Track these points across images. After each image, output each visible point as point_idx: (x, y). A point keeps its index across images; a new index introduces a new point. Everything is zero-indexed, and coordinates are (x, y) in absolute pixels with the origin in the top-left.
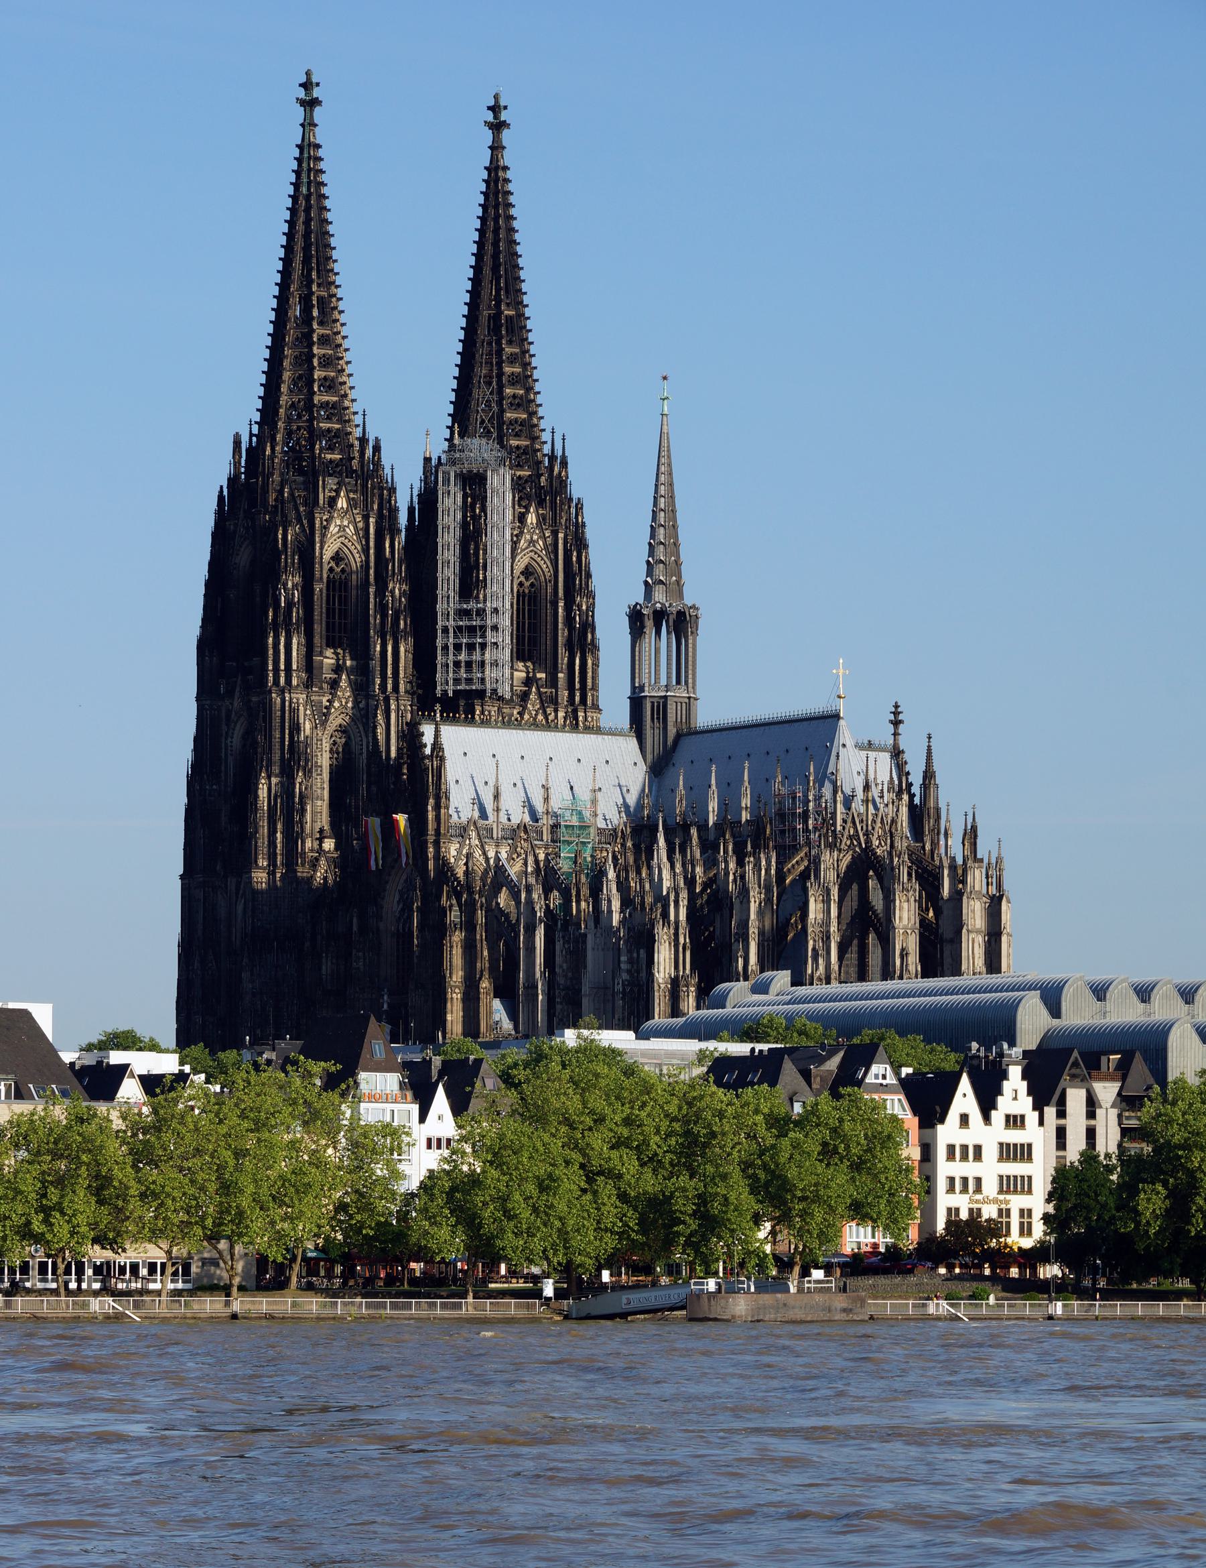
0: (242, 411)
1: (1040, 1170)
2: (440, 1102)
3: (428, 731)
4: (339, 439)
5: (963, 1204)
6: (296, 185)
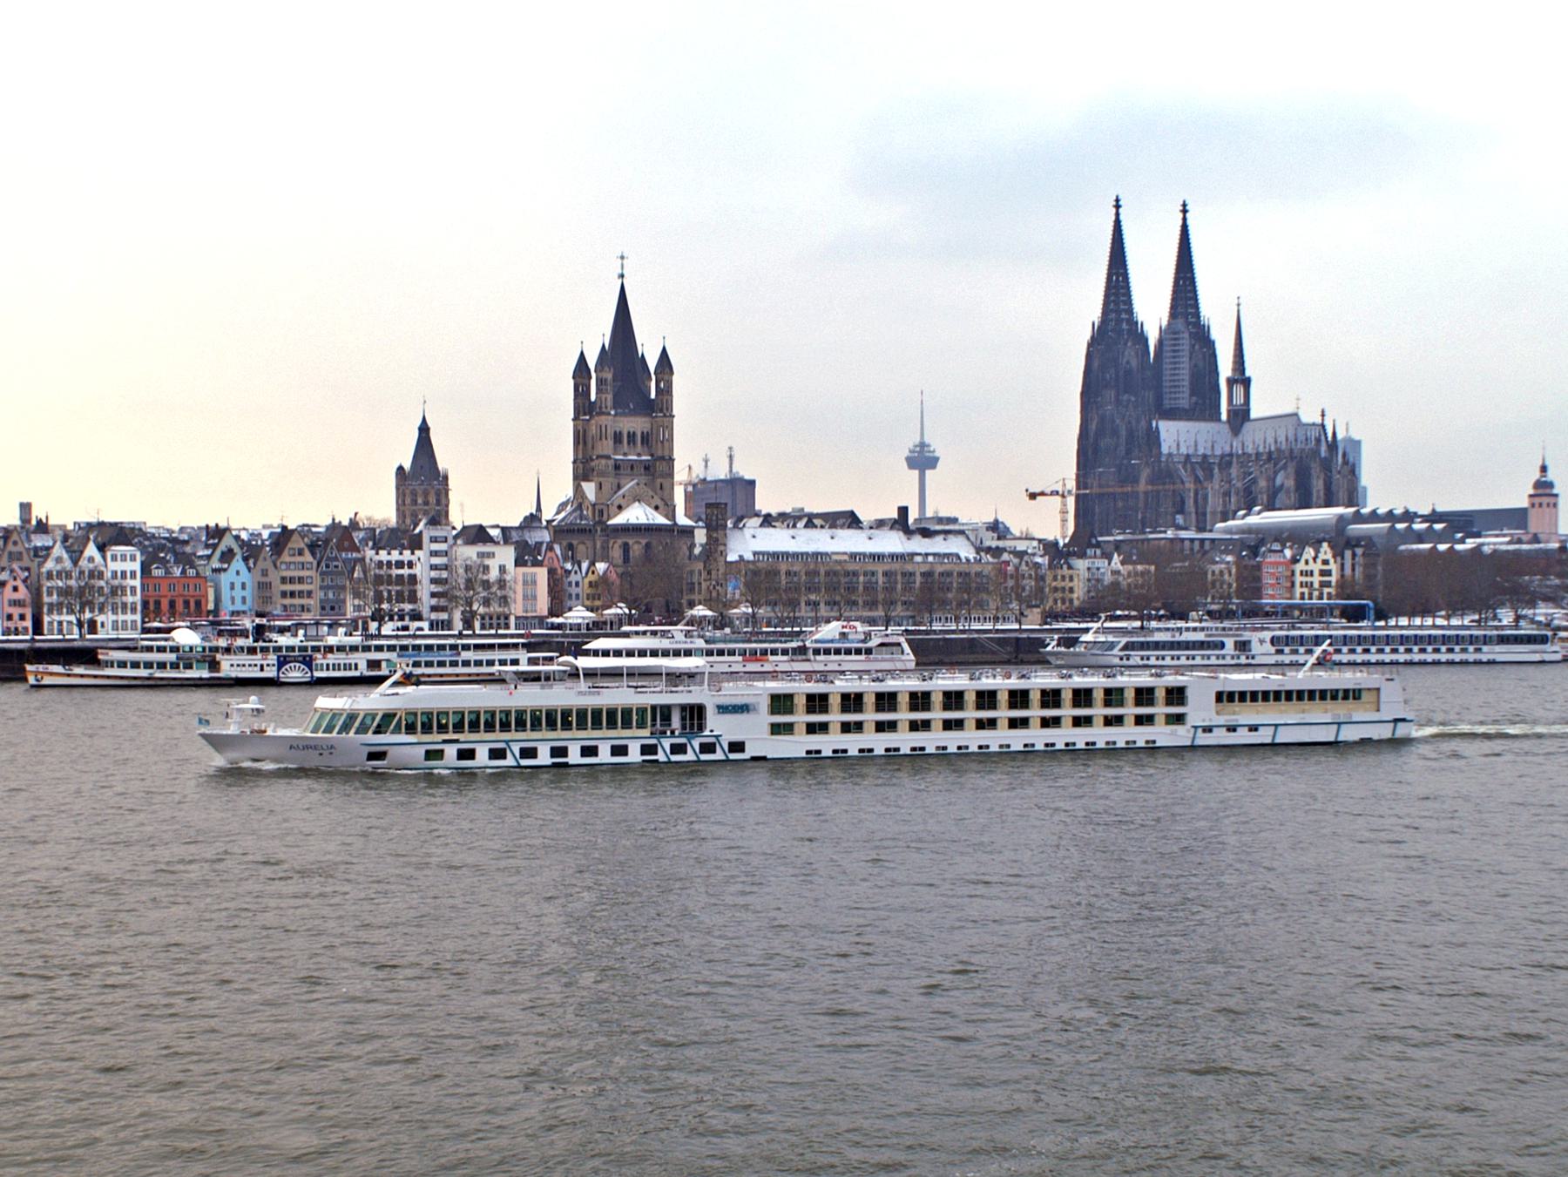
0: (1094, 311)
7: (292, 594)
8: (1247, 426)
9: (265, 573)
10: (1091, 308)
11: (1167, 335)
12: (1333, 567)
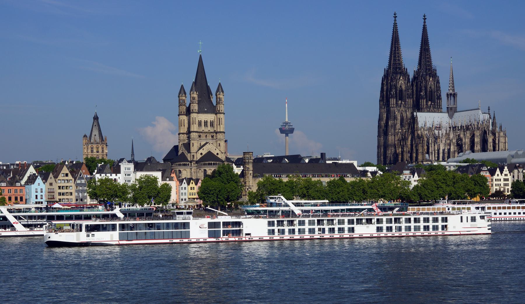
0: (386, 65)
1: (510, 183)
2: (416, 174)
3: (415, 113)
4: (400, 69)
5: (498, 188)
8: (456, 115)
9: (51, 184)
10: (383, 63)
12: (509, 177)
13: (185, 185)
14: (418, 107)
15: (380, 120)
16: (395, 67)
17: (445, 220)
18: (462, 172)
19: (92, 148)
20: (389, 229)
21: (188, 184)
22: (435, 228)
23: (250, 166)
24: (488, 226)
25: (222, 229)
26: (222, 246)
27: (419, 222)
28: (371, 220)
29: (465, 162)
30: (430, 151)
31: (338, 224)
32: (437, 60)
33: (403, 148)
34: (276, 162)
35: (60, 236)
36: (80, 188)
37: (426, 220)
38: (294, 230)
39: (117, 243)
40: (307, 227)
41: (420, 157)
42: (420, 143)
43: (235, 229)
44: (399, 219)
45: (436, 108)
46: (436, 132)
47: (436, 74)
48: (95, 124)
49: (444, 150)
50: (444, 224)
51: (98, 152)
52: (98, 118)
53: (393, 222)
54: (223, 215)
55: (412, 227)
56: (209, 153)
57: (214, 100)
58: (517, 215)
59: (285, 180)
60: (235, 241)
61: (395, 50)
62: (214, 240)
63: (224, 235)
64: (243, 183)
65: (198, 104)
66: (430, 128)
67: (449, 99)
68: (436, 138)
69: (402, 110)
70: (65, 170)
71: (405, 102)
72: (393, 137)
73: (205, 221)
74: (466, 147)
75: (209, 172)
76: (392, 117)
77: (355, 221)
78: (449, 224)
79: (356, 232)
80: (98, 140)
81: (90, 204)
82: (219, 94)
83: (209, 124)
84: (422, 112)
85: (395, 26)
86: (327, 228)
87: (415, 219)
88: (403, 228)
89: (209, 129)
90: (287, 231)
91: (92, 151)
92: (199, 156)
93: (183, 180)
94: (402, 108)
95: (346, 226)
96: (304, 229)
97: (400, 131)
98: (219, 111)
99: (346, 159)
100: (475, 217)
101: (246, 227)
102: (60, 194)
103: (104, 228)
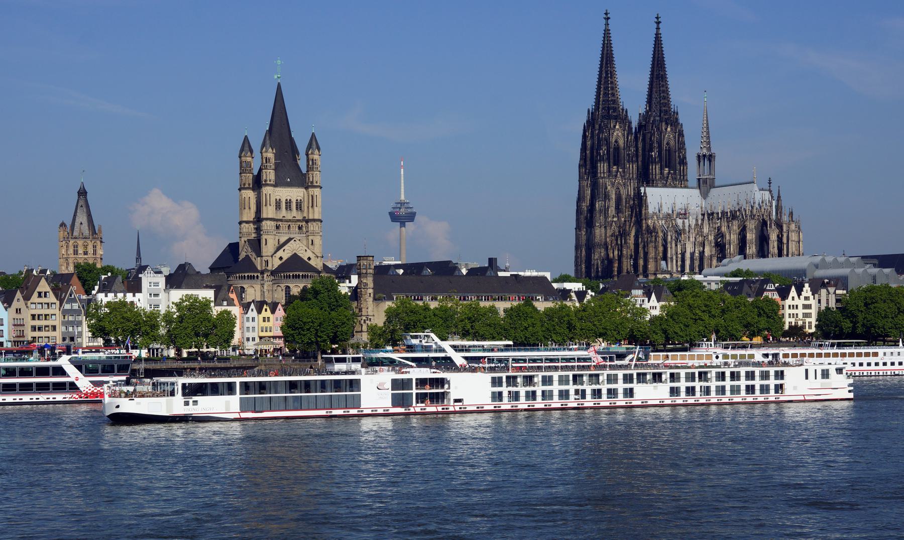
0: (590, 103)
1: (814, 311)
2: (653, 297)
3: (642, 189)
4: (615, 110)
5: (793, 320)
6: (604, 41)
7: (40, 329)
8: (713, 190)
9: (18, 311)
11: (645, 119)
12: (812, 302)
13: (252, 313)
14: (646, 178)
15: (580, 199)
16: (606, 108)
17: (780, 375)
18: (734, 293)
19: (76, 247)
20: (691, 391)
21: (259, 312)
22: (765, 389)
23: (370, 281)
24: (850, 385)
25: (414, 391)
26: (414, 421)
27: (739, 379)
28: (660, 375)
29: (734, 274)
30: (669, 255)
31: (686, 381)
32: (680, 96)
33: (620, 250)
34: (411, 273)
35: (138, 403)
36: (71, 318)
37: (750, 376)
38: (534, 393)
39: (237, 416)
40: (556, 388)
41: (651, 266)
42: (651, 242)
43: (435, 392)
44: (706, 373)
45: (678, 179)
46: (679, 222)
47: (677, 119)
48: (82, 203)
49: (692, 254)
50: (779, 382)
51: (86, 253)
52: (86, 193)
53: (697, 379)
54: (412, 367)
55: (728, 388)
56: (295, 257)
57: (302, 163)
58: (865, 367)
59: (433, 305)
60: (437, 413)
61: (606, 77)
62: (402, 410)
63: (417, 402)
64: (357, 311)
65: (275, 170)
66: (669, 215)
67: (702, 163)
68: (679, 233)
69: (619, 183)
70: (43, 286)
71: (624, 168)
72: (603, 230)
73: (386, 376)
74: (732, 248)
75: (295, 290)
76: (602, 196)
77: (635, 376)
78: (787, 382)
79: (636, 396)
80: (86, 232)
81: (87, 347)
82: (312, 153)
83: (294, 206)
84: (653, 186)
85: (607, 34)
86: (589, 389)
87: (732, 374)
88: (713, 389)
89: (294, 214)
90: (522, 394)
91: (76, 252)
92: (276, 263)
93: (249, 304)
94: (619, 180)
95: (620, 386)
96: (551, 391)
97: (615, 219)
98: (312, 182)
99: (530, 269)
100: (828, 370)
101: (456, 388)
102: (34, 328)
103: (215, 390)
